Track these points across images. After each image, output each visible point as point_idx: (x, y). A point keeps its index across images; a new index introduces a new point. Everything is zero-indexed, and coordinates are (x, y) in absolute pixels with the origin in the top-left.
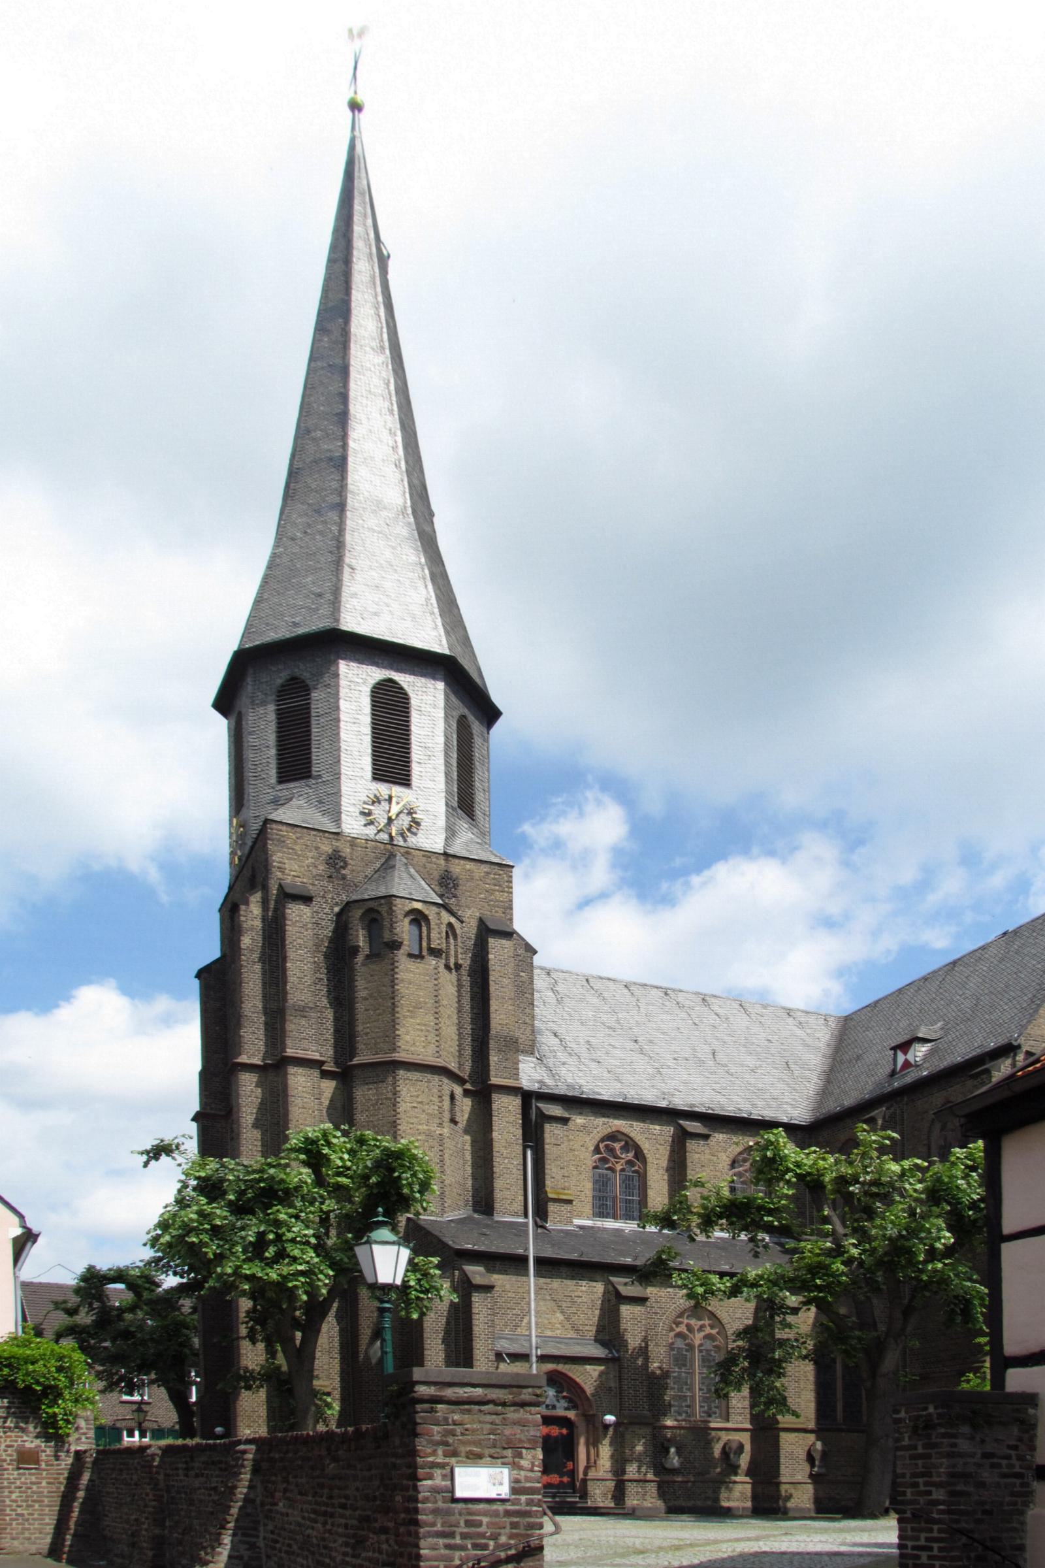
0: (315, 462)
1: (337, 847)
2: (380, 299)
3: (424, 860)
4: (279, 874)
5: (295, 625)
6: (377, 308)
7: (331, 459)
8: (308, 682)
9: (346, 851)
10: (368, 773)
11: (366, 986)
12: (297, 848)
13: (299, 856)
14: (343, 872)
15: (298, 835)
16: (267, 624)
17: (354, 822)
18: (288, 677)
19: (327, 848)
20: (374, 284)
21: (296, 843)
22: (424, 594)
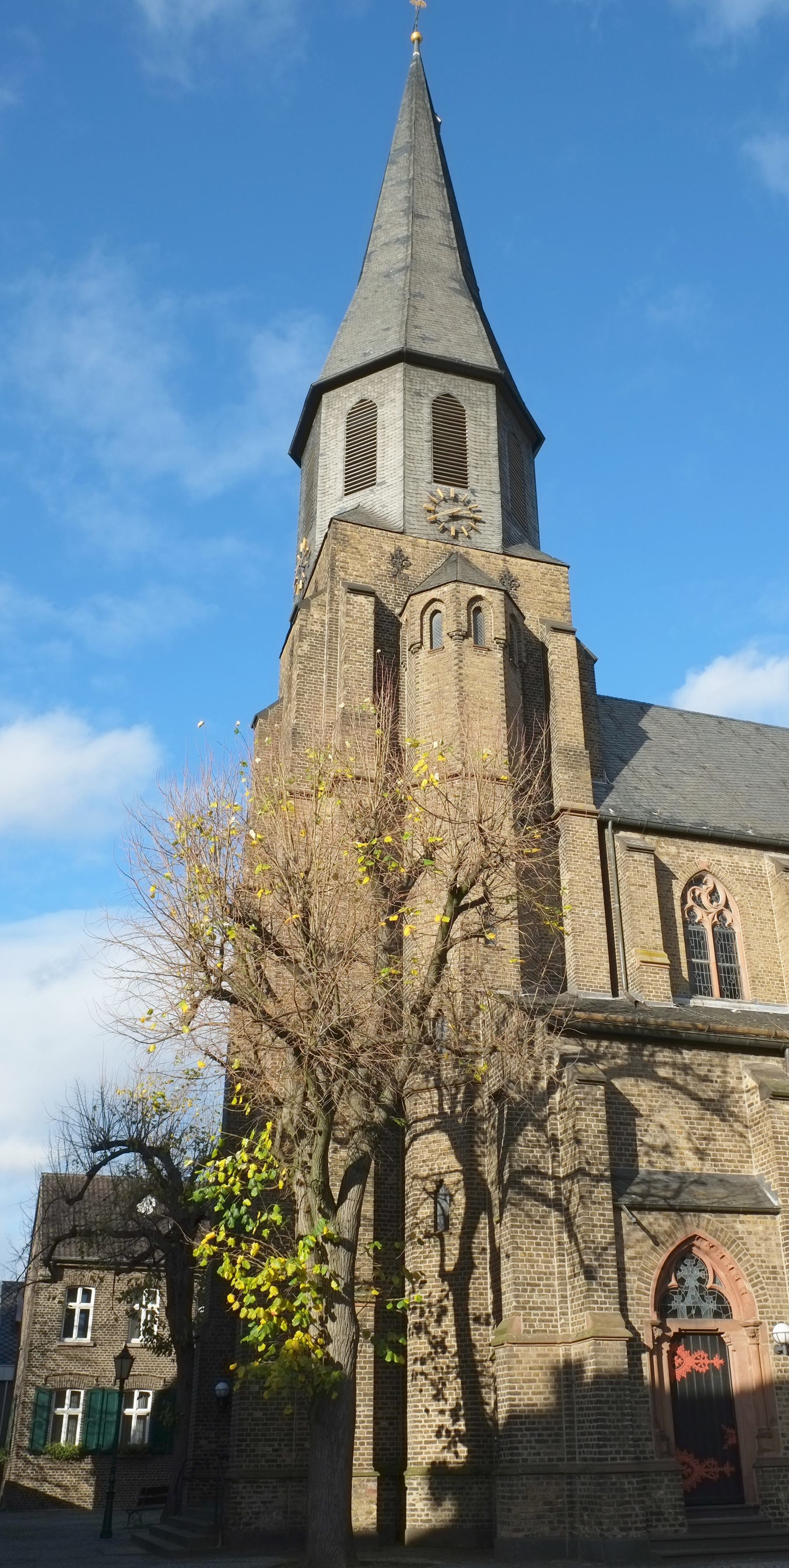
0: (385, 244)
1: (399, 547)
2: (435, 141)
3: (483, 560)
4: (342, 574)
5: (365, 354)
6: (434, 147)
7: (398, 239)
8: (375, 401)
9: (408, 551)
10: (429, 477)
11: (428, 687)
12: (360, 547)
13: (362, 555)
14: (405, 571)
15: (362, 535)
16: (342, 360)
17: (416, 523)
18: (358, 400)
19: (389, 548)
20: (431, 132)
21: (360, 543)
22: (475, 328)
